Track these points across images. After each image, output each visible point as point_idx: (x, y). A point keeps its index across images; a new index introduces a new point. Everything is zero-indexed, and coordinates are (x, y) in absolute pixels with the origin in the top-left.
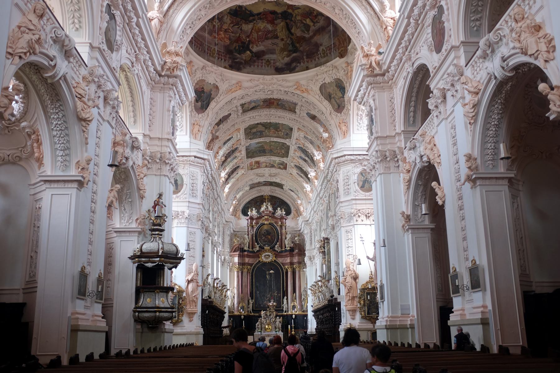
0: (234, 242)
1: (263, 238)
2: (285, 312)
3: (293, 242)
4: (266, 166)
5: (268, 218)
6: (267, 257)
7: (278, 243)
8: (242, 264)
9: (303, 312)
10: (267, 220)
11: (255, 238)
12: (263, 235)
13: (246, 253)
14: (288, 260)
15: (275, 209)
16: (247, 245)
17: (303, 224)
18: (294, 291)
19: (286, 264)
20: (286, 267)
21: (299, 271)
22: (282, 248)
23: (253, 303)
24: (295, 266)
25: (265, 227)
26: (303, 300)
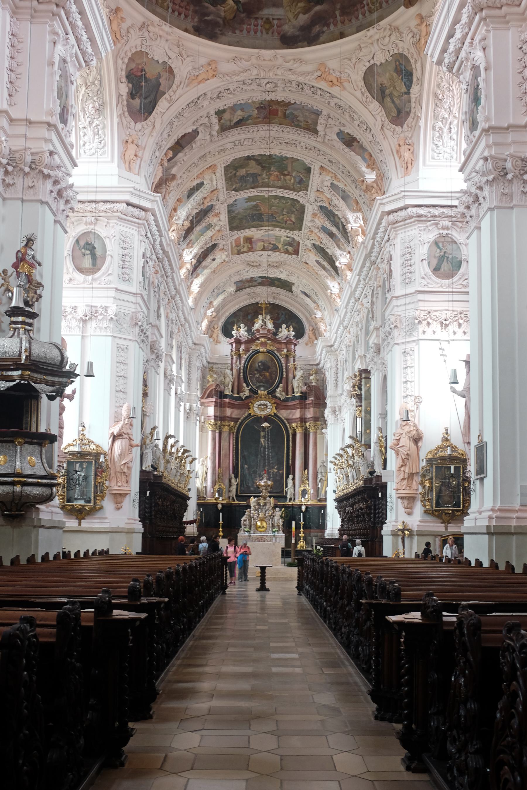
0: (209, 382)
1: (257, 376)
2: (290, 500)
3: (306, 384)
5: (265, 342)
7: (281, 385)
8: (220, 418)
9: (319, 501)
10: (264, 344)
11: (244, 375)
12: (257, 370)
13: (227, 400)
14: (297, 414)
16: (230, 386)
17: (324, 352)
18: (306, 466)
20: (294, 425)
21: (315, 433)
22: (287, 394)
23: (237, 485)
24: (307, 424)
25: (261, 357)
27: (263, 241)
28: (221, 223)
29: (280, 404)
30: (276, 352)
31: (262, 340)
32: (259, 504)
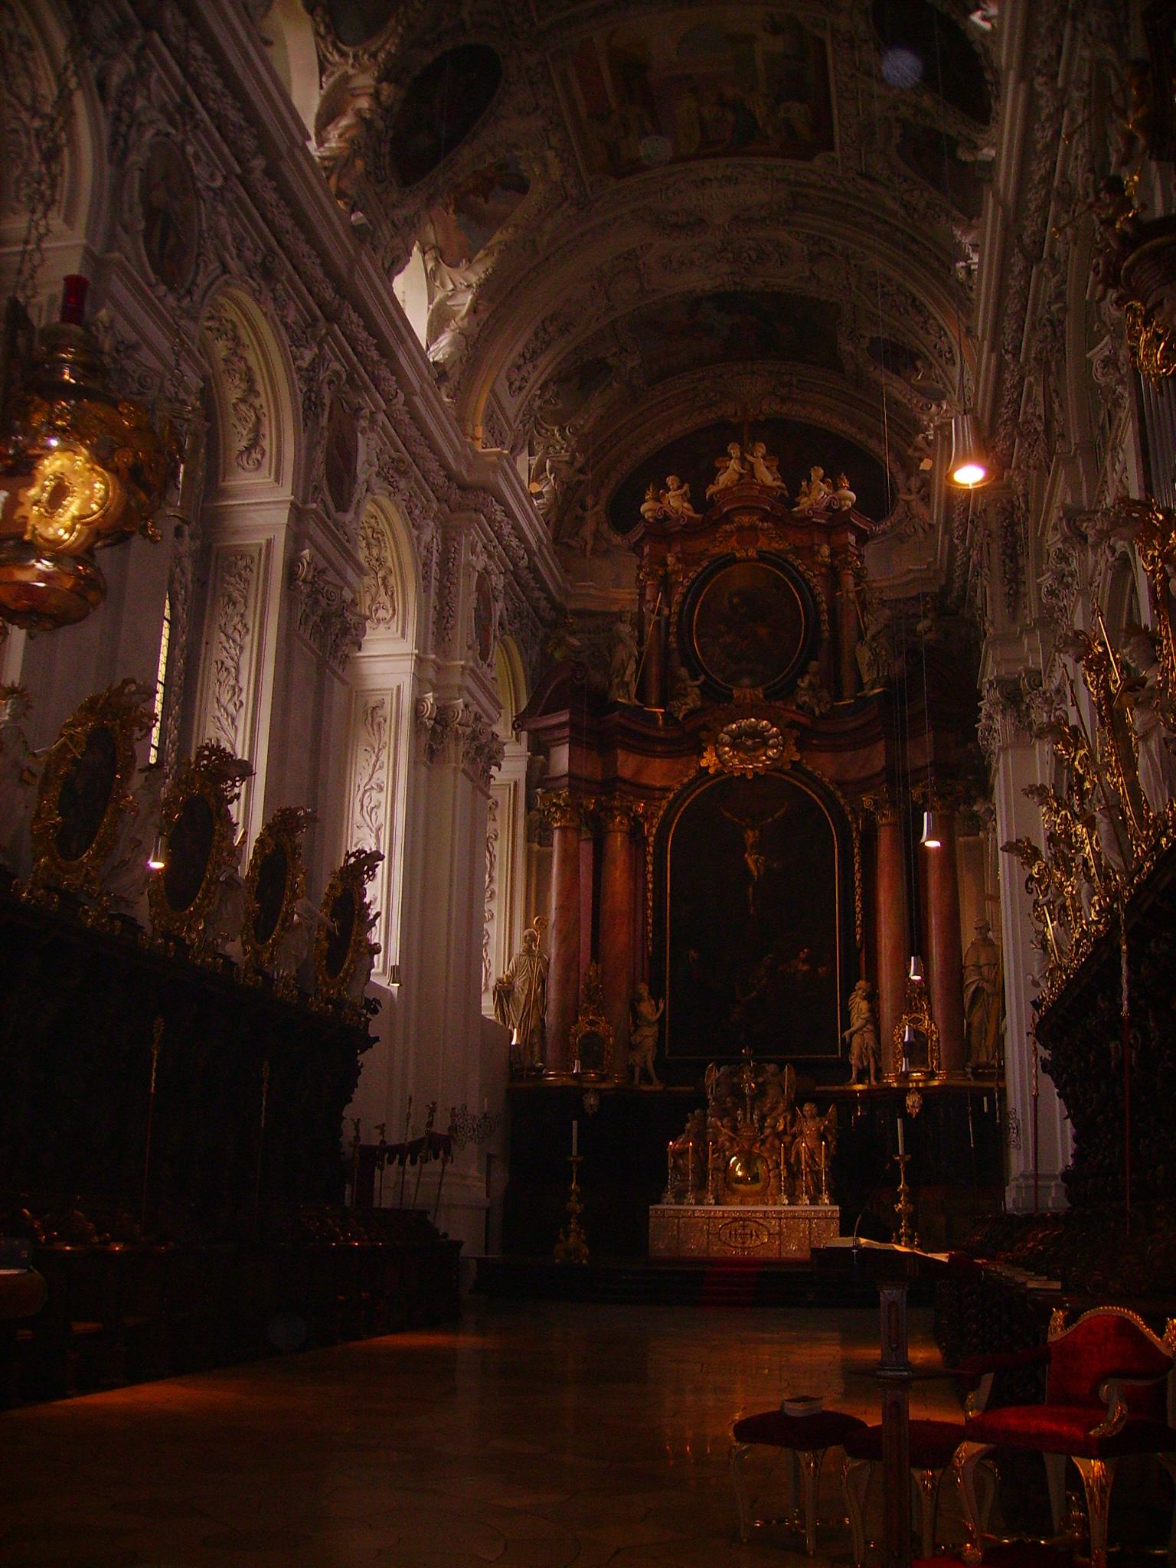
5: (753, 528)
7: (814, 665)
15: (794, 476)
30: (791, 557)
31: (746, 520)
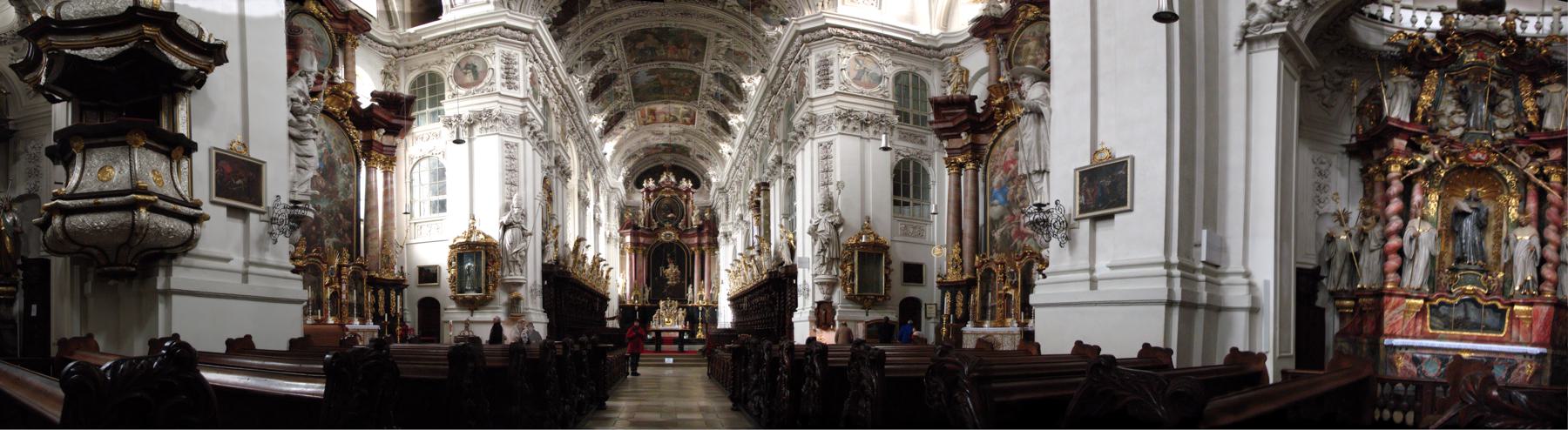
3: (701, 219)
4: (666, 119)
6: (668, 235)
10: (667, 192)
13: (640, 231)
14: (695, 240)
19: (693, 245)
20: (693, 249)
22: (687, 226)
24: (703, 248)
25: (666, 201)
26: (714, 287)
27: (665, 113)
28: (626, 93)
29: (682, 234)
32: (666, 306)
